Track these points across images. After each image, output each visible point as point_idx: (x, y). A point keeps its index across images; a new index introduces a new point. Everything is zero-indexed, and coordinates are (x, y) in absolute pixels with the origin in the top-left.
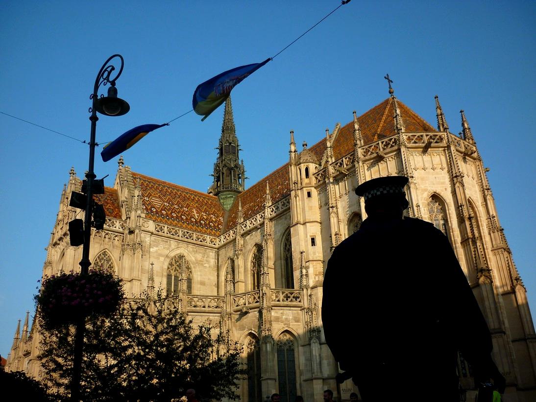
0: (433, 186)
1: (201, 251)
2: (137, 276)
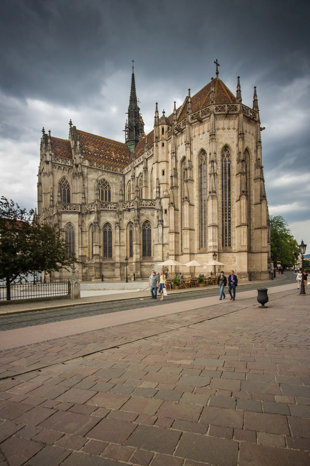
0: (226, 140)
1: (115, 177)
2: (81, 191)
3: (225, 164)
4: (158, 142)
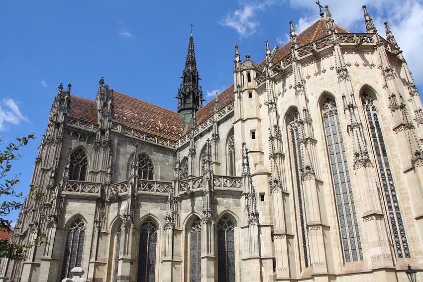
3: (369, 115)
4: (242, 92)
